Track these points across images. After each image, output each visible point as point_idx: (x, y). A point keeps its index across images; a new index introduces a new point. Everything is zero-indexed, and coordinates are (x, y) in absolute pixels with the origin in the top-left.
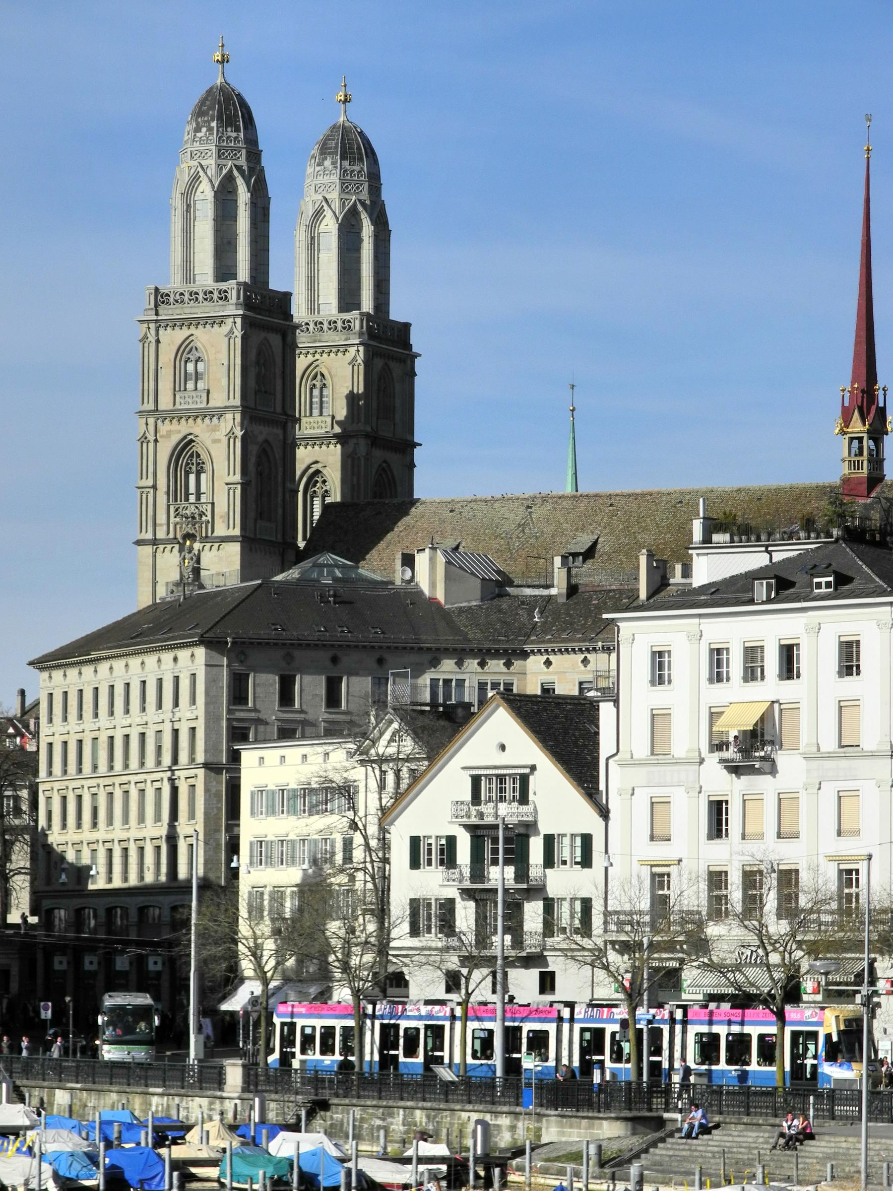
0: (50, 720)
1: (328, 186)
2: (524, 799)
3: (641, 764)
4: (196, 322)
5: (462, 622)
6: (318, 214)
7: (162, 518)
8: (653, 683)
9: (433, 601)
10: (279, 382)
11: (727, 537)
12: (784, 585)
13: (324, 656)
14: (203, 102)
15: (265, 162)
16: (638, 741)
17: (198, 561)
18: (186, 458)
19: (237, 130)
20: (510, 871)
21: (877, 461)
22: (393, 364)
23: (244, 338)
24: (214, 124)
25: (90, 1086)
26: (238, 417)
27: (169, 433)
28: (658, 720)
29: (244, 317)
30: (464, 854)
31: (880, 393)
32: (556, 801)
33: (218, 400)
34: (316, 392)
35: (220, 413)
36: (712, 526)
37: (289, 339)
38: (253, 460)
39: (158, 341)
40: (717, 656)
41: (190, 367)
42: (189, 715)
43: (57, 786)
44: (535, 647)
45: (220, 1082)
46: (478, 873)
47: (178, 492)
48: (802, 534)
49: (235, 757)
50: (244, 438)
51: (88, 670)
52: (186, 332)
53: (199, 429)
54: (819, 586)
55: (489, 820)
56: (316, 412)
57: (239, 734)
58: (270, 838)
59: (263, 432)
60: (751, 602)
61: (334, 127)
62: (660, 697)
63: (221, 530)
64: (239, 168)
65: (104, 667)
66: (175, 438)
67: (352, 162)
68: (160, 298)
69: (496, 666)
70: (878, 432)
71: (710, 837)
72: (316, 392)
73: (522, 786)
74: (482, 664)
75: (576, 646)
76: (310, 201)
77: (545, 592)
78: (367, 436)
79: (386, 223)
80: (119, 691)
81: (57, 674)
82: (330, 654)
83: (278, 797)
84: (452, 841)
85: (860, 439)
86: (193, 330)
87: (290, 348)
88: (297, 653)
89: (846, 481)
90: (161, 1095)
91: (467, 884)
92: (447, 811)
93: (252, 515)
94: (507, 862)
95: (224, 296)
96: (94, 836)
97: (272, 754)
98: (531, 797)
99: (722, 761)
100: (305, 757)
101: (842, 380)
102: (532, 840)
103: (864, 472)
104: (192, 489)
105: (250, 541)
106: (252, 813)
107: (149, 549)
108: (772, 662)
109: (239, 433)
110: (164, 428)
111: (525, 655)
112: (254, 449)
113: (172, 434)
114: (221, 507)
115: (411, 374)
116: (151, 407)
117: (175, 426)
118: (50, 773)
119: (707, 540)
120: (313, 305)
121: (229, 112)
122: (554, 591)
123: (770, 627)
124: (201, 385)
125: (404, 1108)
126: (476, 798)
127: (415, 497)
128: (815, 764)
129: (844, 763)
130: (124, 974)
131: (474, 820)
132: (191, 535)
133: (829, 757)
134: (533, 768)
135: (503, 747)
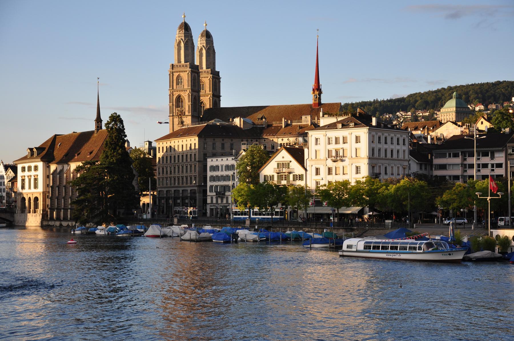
1: (203, 43)
2: (289, 168)
3: (314, 160)
6: (201, 49)
7: (174, 111)
9: (240, 128)
12: (345, 125)
13: (221, 139)
14: (181, 26)
18: (179, 99)
20: (286, 181)
21: (320, 99)
32: (296, 167)
47: (178, 106)
59: (195, 94)
60: (337, 128)
62: (317, 147)
65: (172, 142)
74: (252, 141)
76: (200, 46)
81: (161, 143)
84: (273, 176)
87: (199, 76)
89: (314, 103)
94: (285, 180)
95: (186, 66)
96: (171, 176)
97: (214, 159)
100: (227, 159)
101: (312, 83)
103: (317, 102)
105: (193, 116)
112: (193, 97)
113: (176, 94)
117: (177, 92)
119: (323, 116)
120: (202, 68)
121: (186, 28)
123: (340, 133)
127: (221, 106)
130: (179, 203)
132: (182, 114)
134: (291, 162)
135: (283, 157)
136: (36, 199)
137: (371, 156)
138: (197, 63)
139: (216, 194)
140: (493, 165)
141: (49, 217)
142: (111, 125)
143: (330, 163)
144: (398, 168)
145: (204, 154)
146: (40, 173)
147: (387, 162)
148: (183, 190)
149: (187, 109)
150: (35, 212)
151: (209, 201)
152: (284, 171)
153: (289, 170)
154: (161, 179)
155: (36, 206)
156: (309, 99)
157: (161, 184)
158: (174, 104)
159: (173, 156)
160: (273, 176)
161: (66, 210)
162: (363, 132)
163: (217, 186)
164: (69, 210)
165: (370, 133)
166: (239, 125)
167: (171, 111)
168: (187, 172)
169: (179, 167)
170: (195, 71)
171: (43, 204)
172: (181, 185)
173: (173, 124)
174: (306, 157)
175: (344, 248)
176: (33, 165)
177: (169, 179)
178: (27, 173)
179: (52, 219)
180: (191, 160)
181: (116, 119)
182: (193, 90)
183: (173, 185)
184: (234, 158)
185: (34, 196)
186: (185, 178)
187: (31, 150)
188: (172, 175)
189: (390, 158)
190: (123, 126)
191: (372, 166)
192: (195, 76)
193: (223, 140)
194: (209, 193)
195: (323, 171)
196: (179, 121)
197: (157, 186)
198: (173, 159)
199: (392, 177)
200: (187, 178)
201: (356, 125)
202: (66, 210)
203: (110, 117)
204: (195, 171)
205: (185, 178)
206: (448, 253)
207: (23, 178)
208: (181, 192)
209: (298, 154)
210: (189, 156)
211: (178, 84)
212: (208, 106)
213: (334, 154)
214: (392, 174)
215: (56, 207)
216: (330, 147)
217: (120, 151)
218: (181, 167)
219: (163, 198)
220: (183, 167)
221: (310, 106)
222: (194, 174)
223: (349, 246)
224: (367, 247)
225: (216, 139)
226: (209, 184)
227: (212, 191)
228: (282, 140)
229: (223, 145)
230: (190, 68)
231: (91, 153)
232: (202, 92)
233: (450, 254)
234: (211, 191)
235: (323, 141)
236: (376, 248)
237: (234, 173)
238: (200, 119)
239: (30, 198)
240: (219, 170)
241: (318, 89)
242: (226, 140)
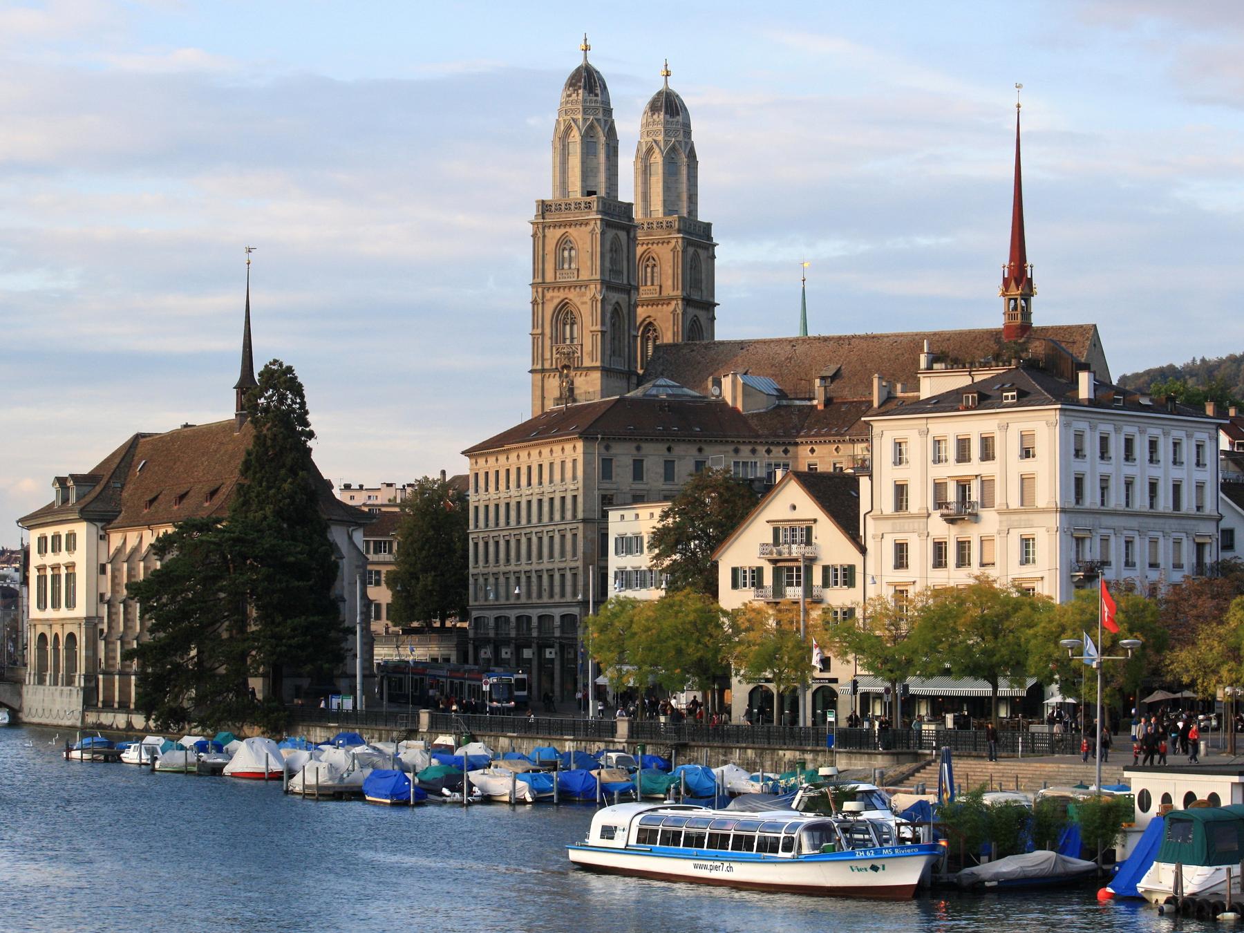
0: (477, 491)
1: (656, 132)
2: (809, 542)
3: (887, 518)
4: (570, 224)
5: (753, 423)
7: (547, 355)
8: (895, 464)
9: (735, 410)
10: (625, 263)
11: (943, 366)
12: (983, 398)
13: (662, 447)
15: (615, 116)
16: (887, 503)
17: (572, 383)
18: (565, 315)
19: (596, 95)
21: (1026, 313)
22: (700, 251)
23: (603, 233)
24: (580, 91)
25: (523, 735)
26: (599, 287)
27: (552, 298)
28: (901, 491)
29: (602, 220)
30: (768, 580)
31: (1029, 269)
32: (831, 544)
33: (585, 275)
34: (649, 270)
35: (584, 285)
36: (935, 358)
37: (632, 235)
38: (609, 315)
39: (544, 236)
41: (566, 253)
42: (572, 487)
43: (481, 535)
44: (804, 440)
45: (613, 730)
46: (778, 590)
47: (558, 338)
48: (993, 363)
49: (605, 515)
50: (602, 301)
51: (502, 458)
52: (563, 230)
53: (572, 295)
54: (1007, 398)
55: (786, 556)
56: (649, 283)
57: (608, 501)
58: (629, 569)
59: (615, 297)
61: (660, 93)
63: (587, 363)
64: (598, 120)
65: (513, 456)
66: (556, 301)
67: (672, 115)
68: (544, 208)
69: (777, 452)
70: (1028, 294)
71: (935, 566)
72: (649, 270)
74: (769, 451)
75: (832, 439)
77: (809, 403)
78: (683, 299)
79: (695, 157)
80: (524, 471)
82: (667, 446)
83: (634, 542)
84: (758, 572)
85: (1016, 300)
86: (568, 229)
87: (632, 241)
89: (1007, 327)
90: (572, 740)
91: (771, 599)
92: (757, 551)
93: (608, 352)
95: (588, 206)
98: (814, 541)
99: (942, 515)
102: (815, 568)
103: (1019, 321)
104: (568, 335)
105: (606, 371)
106: (616, 553)
107: (539, 376)
108: (975, 450)
109: (599, 298)
110: (549, 295)
111: (796, 444)
112: (609, 308)
113: (555, 298)
114: (588, 347)
115: (713, 257)
116: (540, 280)
117: (556, 293)
118: (476, 526)
119: (930, 368)
122: (815, 402)
123: (974, 426)
124: (573, 266)
125: (740, 748)
127: (716, 339)
128: (1004, 517)
129: (1024, 517)
131: (775, 556)
132: (568, 366)
133: (1015, 512)
134: (815, 521)
135: (794, 507)
136: (71, 637)
137: (1071, 503)
138: (627, 192)
141: (101, 698)
142: (262, 400)
143: (939, 528)
144: (1177, 543)
146: (80, 557)
147: (1134, 523)
148: (540, 618)
149: (588, 347)
150: (70, 682)
152: (794, 555)
153: (808, 551)
154: (481, 580)
155: (71, 667)
156: (991, 315)
157: (481, 595)
158: (548, 330)
160: (758, 572)
161: (124, 674)
162: (1044, 425)
164: (117, 677)
165: (1066, 426)
166: (730, 403)
167: (538, 355)
168: (551, 556)
170: (617, 219)
171: (87, 657)
173: (543, 398)
174: (864, 506)
175: (594, 838)
176: (63, 530)
177: (491, 580)
178: (50, 559)
179: (108, 706)
180: (563, 518)
181: (283, 379)
182: (607, 285)
185: (69, 629)
186: (545, 577)
187: (61, 481)
188: (512, 568)
190: (303, 404)
191: (1076, 539)
192: (616, 237)
193: (638, 448)
195: (920, 553)
196: (561, 386)
197: (471, 603)
198: (513, 514)
199: (1153, 575)
201: (1024, 397)
202: (124, 674)
204: (574, 554)
205: (545, 577)
206: (868, 865)
207: (42, 573)
208: (535, 622)
209: (839, 497)
210: (557, 503)
211: (559, 266)
212: (667, 338)
213: (952, 495)
214: (1129, 564)
215: (118, 666)
217: (286, 486)
219: (486, 641)
221: (994, 335)
222: (573, 565)
223: (608, 832)
224: (646, 836)
225: (644, 445)
229: (669, 466)
230: (598, 212)
231: (213, 493)
232: (645, 293)
233: (875, 868)
235: (917, 449)
236: (671, 838)
238: (634, 380)
239: (56, 636)
240: (642, 552)
241: (1019, 278)
242: (679, 449)
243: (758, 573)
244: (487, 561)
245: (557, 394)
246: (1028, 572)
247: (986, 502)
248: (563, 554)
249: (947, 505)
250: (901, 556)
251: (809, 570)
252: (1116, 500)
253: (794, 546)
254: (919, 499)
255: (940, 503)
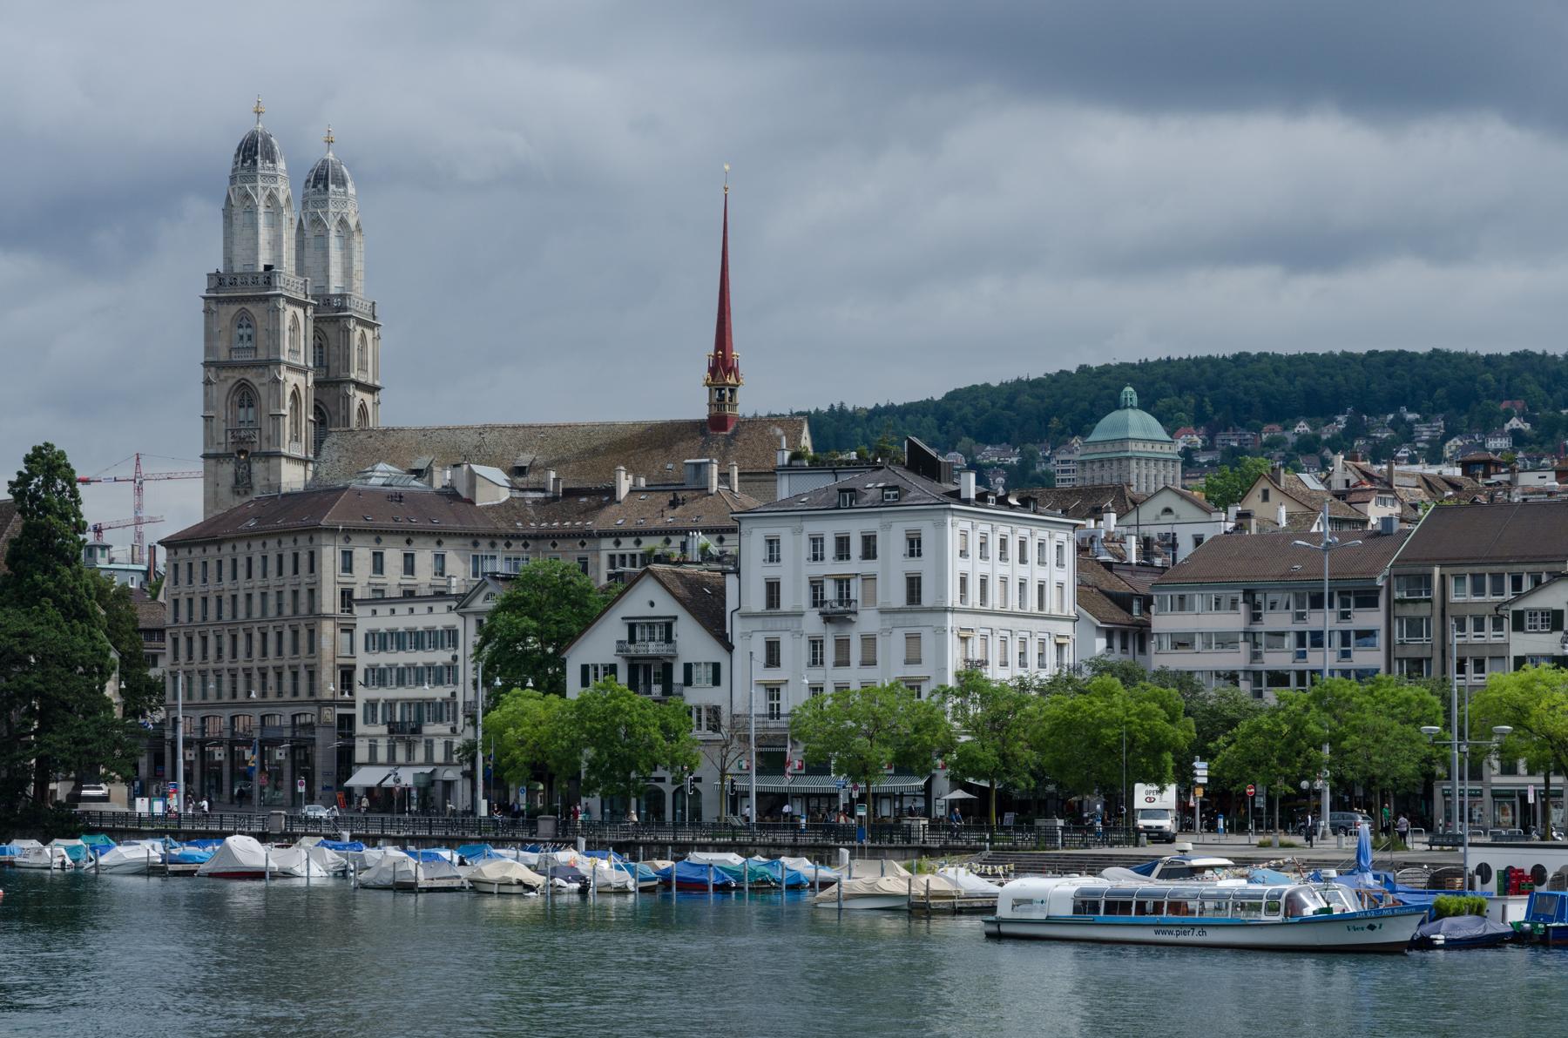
2: (668, 639)
16: (757, 602)
27: (226, 379)
28: (773, 588)
40: (817, 541)
53: (250, 375)
73: (667, 628)
82: (404, 539)
88: (383, 538)
96: (219, 665)
106: (367, 649)
108: (856, 548)
117: (229, 373)
118: (176, 621)
126: (632, 639)
129: (909, 616)
133: (899, 611)
134: (676, 618)
135: (652, 604)
139: (391, 731)
140: (1345, 635)
145: (343, 593)
151: (361, 754)
156: (697, 407)
159: (226, 597)
163: (390, 704)
169: (249, 636)
172: (287, 697)
174: (731, 603)
183: (226, 699)
184: (454, 604)
189: (1036, 610)
194: (360, 727)
195: (794, 651)
200: (279, 675)
203: (28, 460)
213: (830, 592)
216: (818, 570)
218: (257, 636)
220: (264, 635)
226: (362, 694)
227: (374, 721)
228: (618, 543)
233: (1372, 927)
234: (370, 718)
237: (455, 658)
243: (612, 669)
244: (190, 658)
245: (231, 480)
246: (913, 671)
247: (870, 598)
248: (295, 650)
249: (823, 603)
250: (773, 656)
251: (668, 669)
252: (994, 601)
253: (651, 644)
254: (795, 596)
255: (817, 600)
